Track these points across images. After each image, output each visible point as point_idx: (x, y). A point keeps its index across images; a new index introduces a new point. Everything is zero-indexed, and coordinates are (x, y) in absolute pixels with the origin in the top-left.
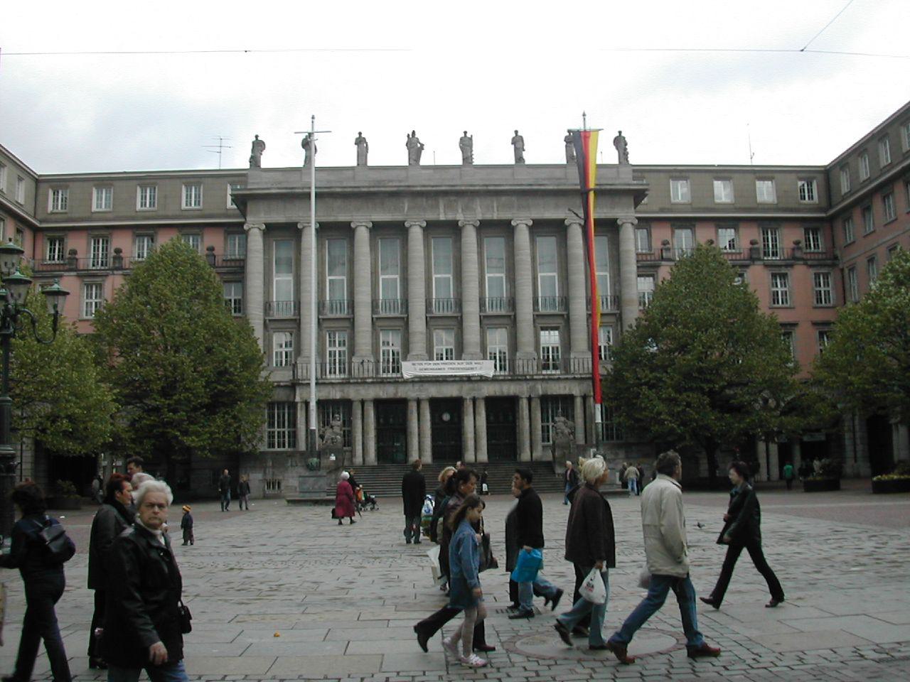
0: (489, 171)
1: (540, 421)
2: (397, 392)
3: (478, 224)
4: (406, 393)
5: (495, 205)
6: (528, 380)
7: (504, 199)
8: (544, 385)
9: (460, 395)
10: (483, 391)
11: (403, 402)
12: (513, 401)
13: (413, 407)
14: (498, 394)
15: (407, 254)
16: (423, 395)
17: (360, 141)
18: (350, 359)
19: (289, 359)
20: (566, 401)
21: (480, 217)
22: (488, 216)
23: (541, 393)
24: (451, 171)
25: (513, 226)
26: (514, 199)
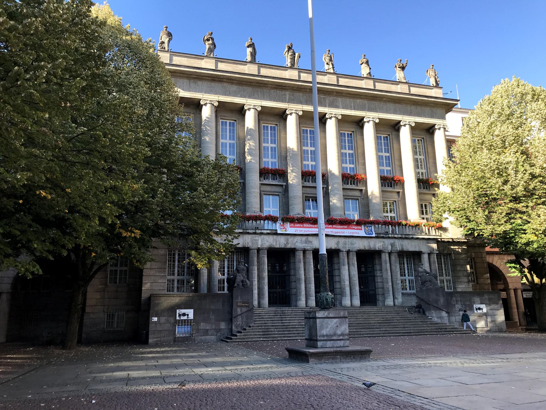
2: (287, 243)
4: (295, 244)
7: (358, 101)
9: (337, 248)
10: (355, 245)
11: (292, 251)
12: (378, 253)
13: (300, 255)
14: (367, 248)
16: (308, 247)
19: (411, 285)
23: (399, 249)
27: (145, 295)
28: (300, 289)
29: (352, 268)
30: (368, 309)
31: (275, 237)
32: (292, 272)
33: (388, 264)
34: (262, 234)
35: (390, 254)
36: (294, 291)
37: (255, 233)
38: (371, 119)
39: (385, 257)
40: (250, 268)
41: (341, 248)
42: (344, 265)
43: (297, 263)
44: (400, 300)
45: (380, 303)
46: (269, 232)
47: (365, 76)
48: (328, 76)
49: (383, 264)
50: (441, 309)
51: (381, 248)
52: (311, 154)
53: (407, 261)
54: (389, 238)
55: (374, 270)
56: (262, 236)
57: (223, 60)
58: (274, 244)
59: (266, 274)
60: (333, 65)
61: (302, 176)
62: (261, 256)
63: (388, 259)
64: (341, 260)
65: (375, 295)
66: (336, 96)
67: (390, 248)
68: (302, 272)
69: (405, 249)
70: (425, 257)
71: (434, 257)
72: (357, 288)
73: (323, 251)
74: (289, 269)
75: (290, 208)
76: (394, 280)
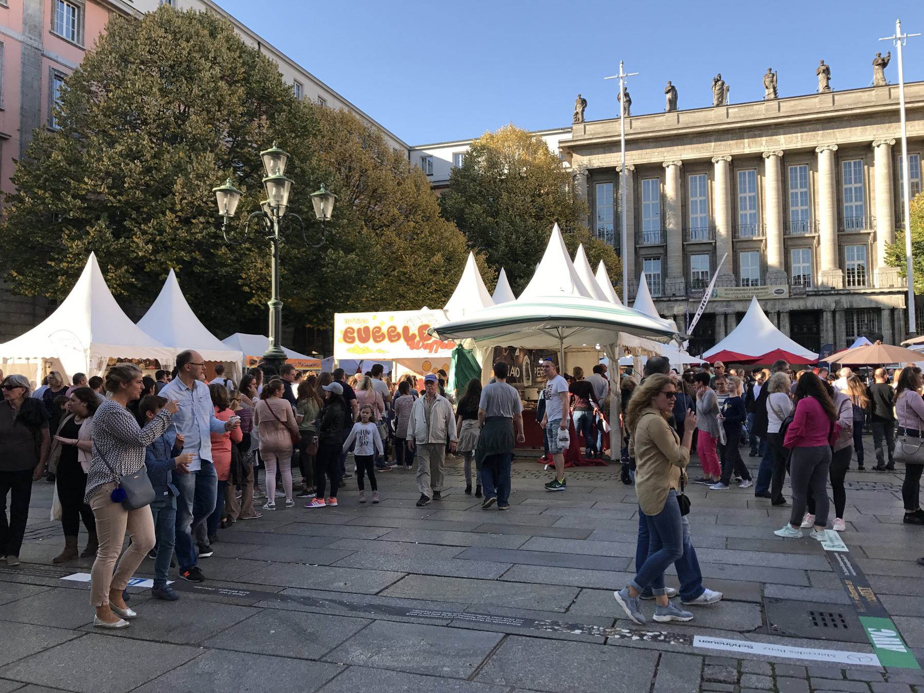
1: (844, 334)
6: (832, 294)
10: (787, 306)
14: (802, 308)
16: (730, 310)
18: (664, 280)
33: (830, 325)
35: (834, 313)
37: (669, 301)
38: (825, 148)
39: (827, 316)
47: (821, 91)
48: (767, 104)
52: (802, 196)
53: (858, 318)
54: (832, 294)
57: (638, 117)
60: (774, 88)
67: (833, 306)
69: (855, 306)
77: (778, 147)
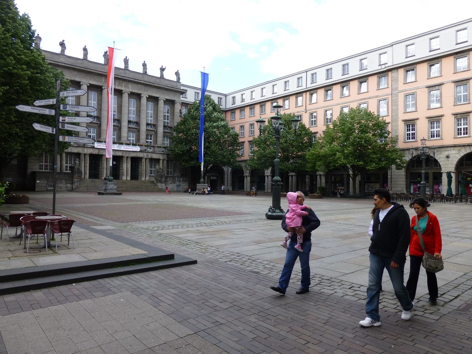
0: (136, 74)
3: (130, 93)
5: (136, 87)
6: (146, 152)
7: (139, 85)
8: (151, 154)
9: (122, 155)
12: (140, 159)
14: (136, 156)
15: (101, 100)
17: (85, 50)
20: (158, 160)
21: (131, 90)
22: (134, 91)
23: (150, 157)
24: (121, 70)
25: (102, 89)
26: (143, 86)
27: (29, 171)
28: (104, 172)
29: (128, 164)
30: (132, 181)
31: (93, 149)
32: (100, 165)
33: (145, 163)
34: (87, 147)
35: (146, 159)
36: (100, 173)
39: (144, 160)
40: (81, 162)
41: (124, 156)
42: (125, 163)
43: (103, 161)
44: (147, 178)
45: (139, 179)
46: (90, 147)
49: (142, 163)
50: (162, 183)
51: (142, 156)
54: (146, 152)
55: (138, 165)
56: (87, 148)
58: (93, 152)
59: (88, 165)
61: (128, 122)
62: (86, 157)
63: (144, 161)
64: (123, 161)
65: (138, 176)
66: (128, 82)
67: (146, 157)
68: (105, 165)
70: (161, 161)
71: (165, 162)
72: (130, 173)
73: (109, 155)
74: (99, 163)
75: (102, 135)
76: (146, 170)
77: (128, 90)
